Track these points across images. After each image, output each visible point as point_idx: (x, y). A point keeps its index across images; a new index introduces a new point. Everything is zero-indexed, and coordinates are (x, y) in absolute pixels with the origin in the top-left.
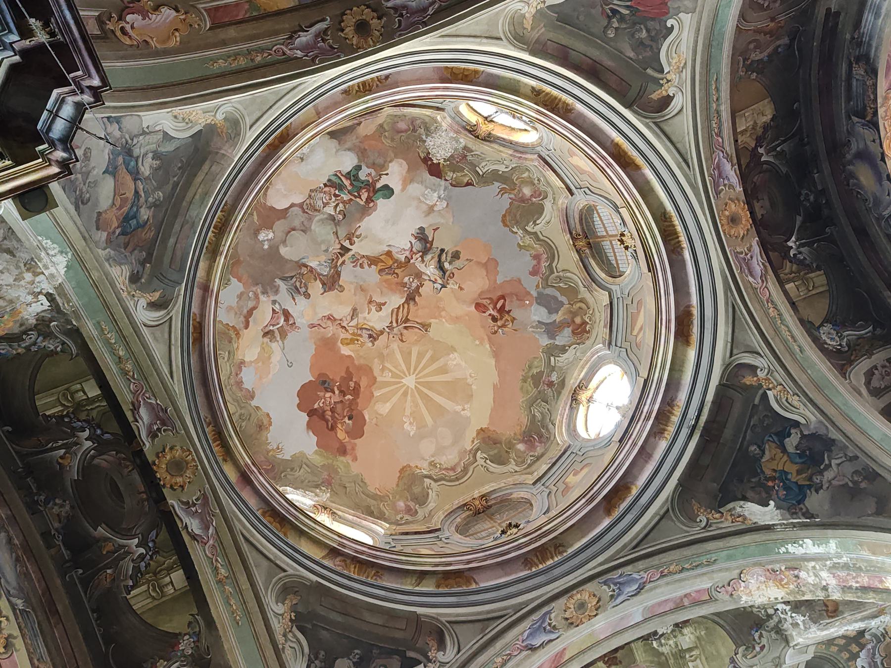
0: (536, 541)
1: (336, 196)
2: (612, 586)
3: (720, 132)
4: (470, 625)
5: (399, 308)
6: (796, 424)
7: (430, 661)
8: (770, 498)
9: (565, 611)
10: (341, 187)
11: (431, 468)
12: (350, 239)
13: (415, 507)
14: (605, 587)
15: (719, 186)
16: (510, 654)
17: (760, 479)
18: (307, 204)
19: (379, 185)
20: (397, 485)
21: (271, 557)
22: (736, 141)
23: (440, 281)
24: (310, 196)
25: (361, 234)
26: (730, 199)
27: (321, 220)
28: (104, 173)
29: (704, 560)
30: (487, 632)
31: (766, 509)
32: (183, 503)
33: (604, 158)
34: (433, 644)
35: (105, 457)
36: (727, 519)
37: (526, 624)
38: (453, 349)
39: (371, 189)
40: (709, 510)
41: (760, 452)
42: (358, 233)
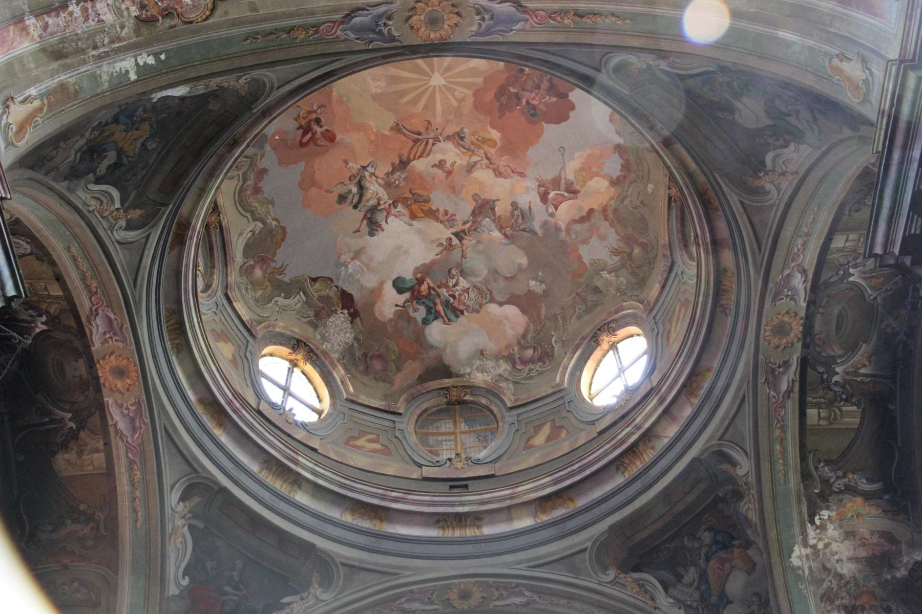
1: (453, 296)
2: (386, 32)
3: (131, 463)
5: (420, 157)
6: (98, 181)
10: (447, 304)
12: (451, 245)
14: (396, 34)
15: (135, 410)
18: (486, 299)
19: (407, 295)
21: (745, 217)
22: (107, 444)
23: (367, 174)
24: (481, 306)
25: (437, 246)
26: (123, 394)
27: (475, 275)
28: (732, 602)
29: (260, 42)
32: (795, 301)
33: (235, 411)
35: (832, 354)
38: (375, 97)
39: (416, 293)
42: (440, 248)
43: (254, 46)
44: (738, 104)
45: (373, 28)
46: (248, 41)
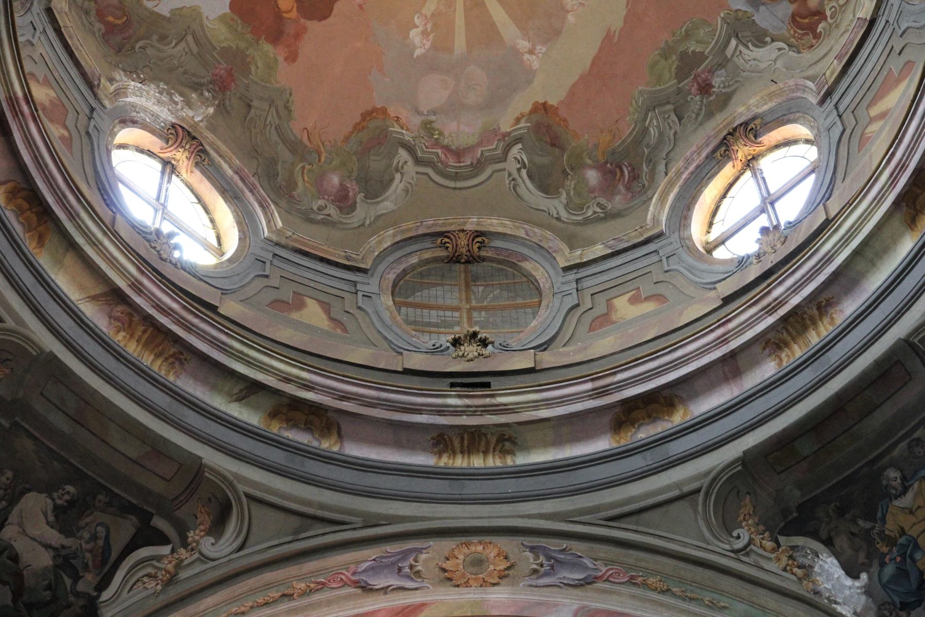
0: (474, 414)
4: (281, 516)
7: (185, 544)
8: (866, 567)
9: (448, 559)
11: (422, 133)
13: (355, 195)
16: (323, 584)
17: (874, 527)
20: (347, 139)
29: (707, 597)
30: (303, 535)
31: (848, 582)
34: (206, 520)
36: (779, 560)
37: (371, 553)
40: (761, 528)
41: (900, 489)
43: (716, 596)
44: (54, 537)
45: (556, 564)
46: (722, 604)
